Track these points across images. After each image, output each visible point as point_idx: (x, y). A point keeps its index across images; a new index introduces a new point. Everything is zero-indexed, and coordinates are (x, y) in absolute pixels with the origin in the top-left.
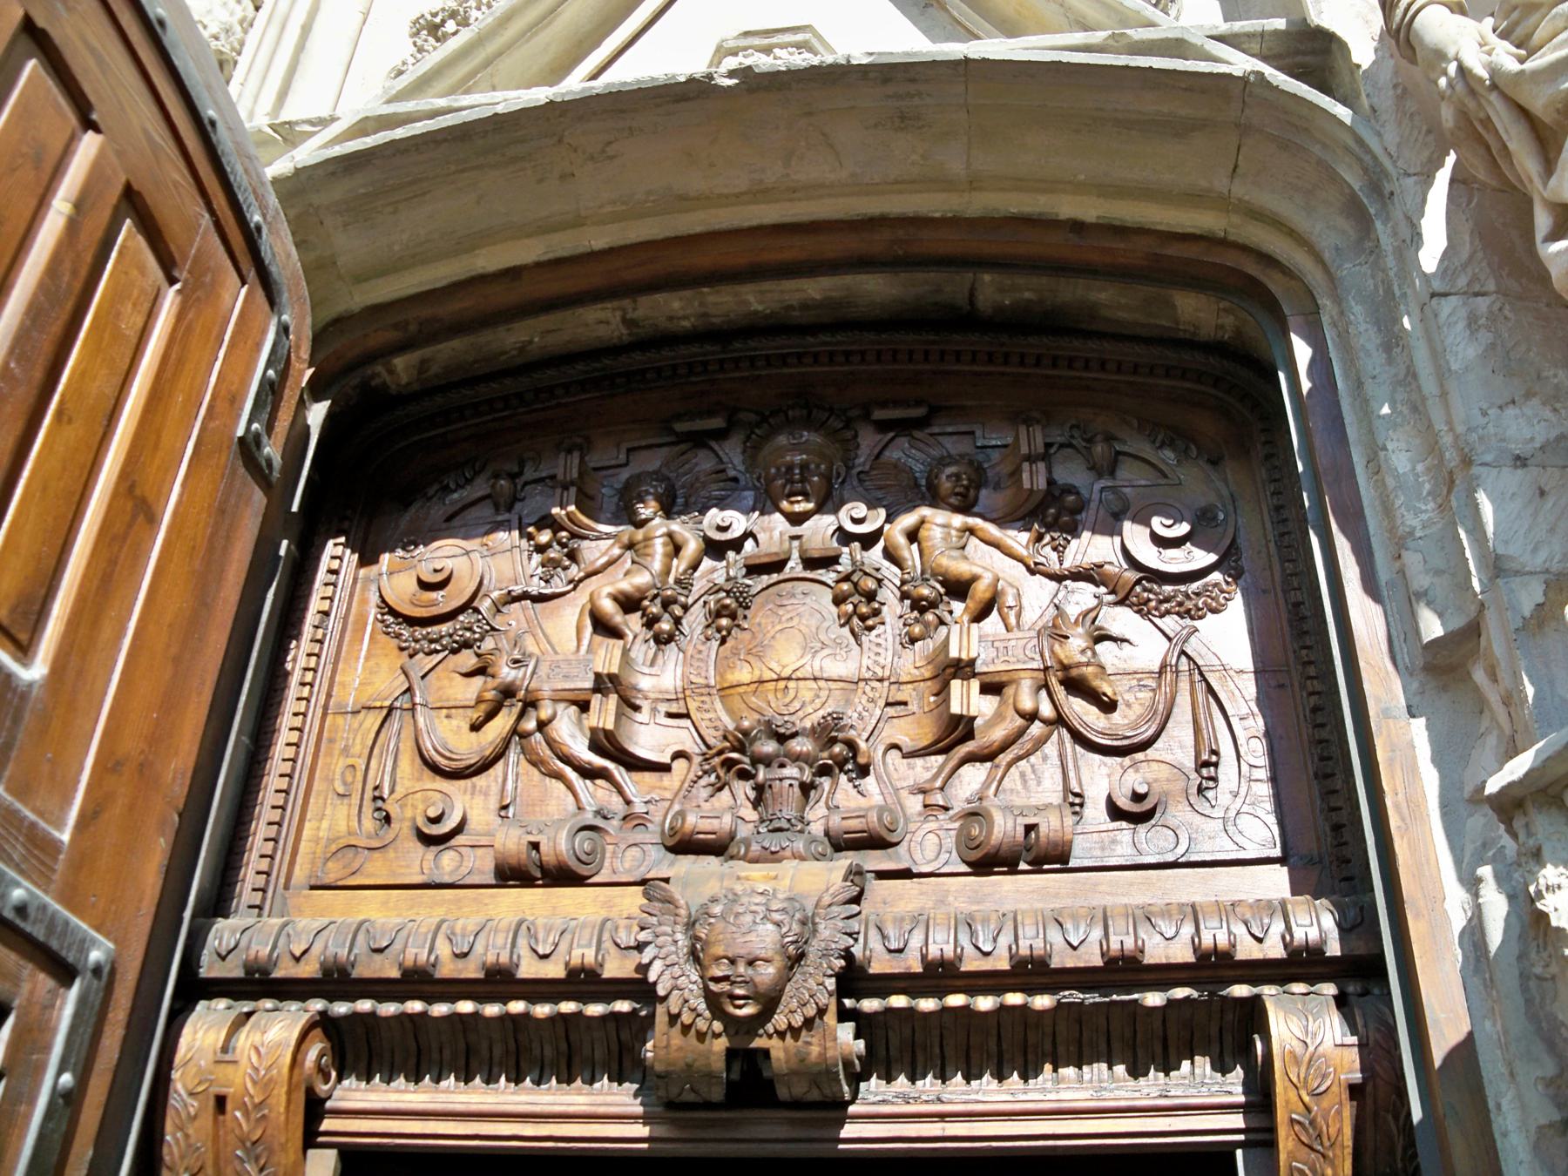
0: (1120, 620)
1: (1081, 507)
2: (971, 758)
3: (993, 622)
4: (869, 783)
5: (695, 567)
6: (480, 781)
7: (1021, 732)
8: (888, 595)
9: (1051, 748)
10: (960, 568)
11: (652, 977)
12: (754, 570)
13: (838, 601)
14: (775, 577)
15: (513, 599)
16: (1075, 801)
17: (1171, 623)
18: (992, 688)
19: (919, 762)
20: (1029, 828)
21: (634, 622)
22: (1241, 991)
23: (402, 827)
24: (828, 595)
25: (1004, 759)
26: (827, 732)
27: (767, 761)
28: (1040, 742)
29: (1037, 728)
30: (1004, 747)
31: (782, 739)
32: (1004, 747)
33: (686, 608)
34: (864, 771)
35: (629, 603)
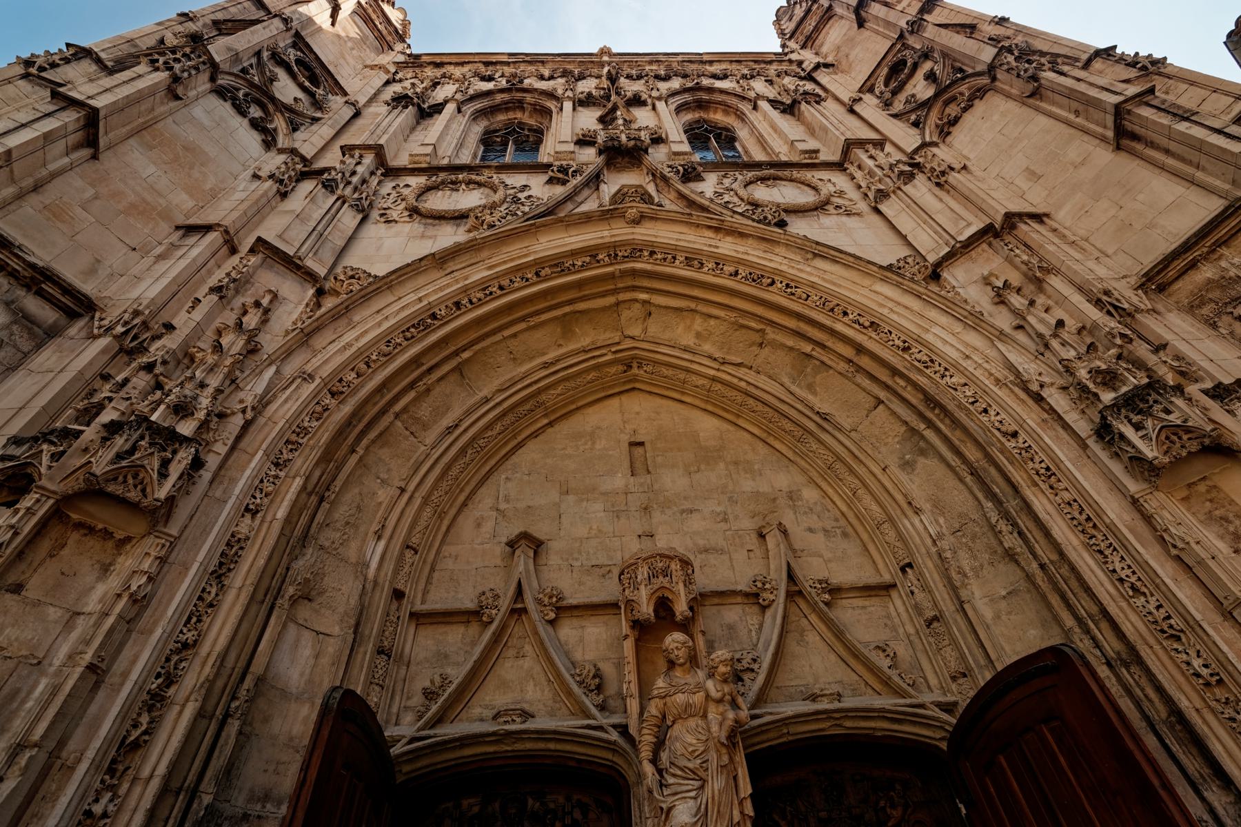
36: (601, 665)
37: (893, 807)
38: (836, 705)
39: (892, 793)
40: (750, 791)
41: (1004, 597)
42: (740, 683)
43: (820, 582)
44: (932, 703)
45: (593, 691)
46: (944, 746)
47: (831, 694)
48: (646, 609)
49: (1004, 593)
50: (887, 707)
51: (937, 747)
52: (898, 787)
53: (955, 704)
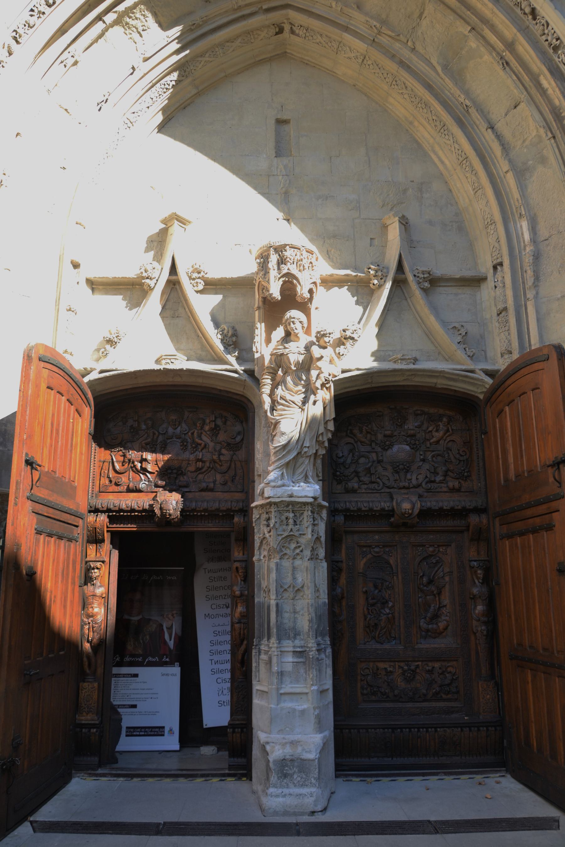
0: (224, 451)
1: (220, 430)
2: (200, 473)
3: (204, 451)
4: (185, 477)
5: (158, 437)
6: (125, 474)
7: (207, 470)
8: (189, 444)
9: (212, 472)
10: (200, 442)
11: (156, 511)
12: (168, 439)
13: (181, 446)
14: (171, 440)
15: (128, 442)
16: (214, 482)
17: (232, 453)
18: (203, 462)
19: (192, 473)
20: (207, 486)
21: (148, 446)
22: (232, 514)
23: (113, 482)
24: (179, 444)
25: (205, 473)
26: (179, 468)
27: (170, 474)
28: (210, 471)
29: (210, 469)
30: (205, 472)
31: (172, 470)
32: (205, 472)
33: (156, 445)
34: (185, 475)
35: (147, 444)
36: (237, 327)
37: (437, 431)
38: (412, 366)
39: (440, 423)
40: (333, 416)
41: (558, 299)
42: (342, 347)
43: (423, 273)
44: (481, 370)
45: (231, 345)
46: (481, 397)
47: (409, 359)
48: (275, 290)
49: (559, 296)
50: (446, 370)
51: (477, 397)
52: (445, 419)
53: (498, 371)
